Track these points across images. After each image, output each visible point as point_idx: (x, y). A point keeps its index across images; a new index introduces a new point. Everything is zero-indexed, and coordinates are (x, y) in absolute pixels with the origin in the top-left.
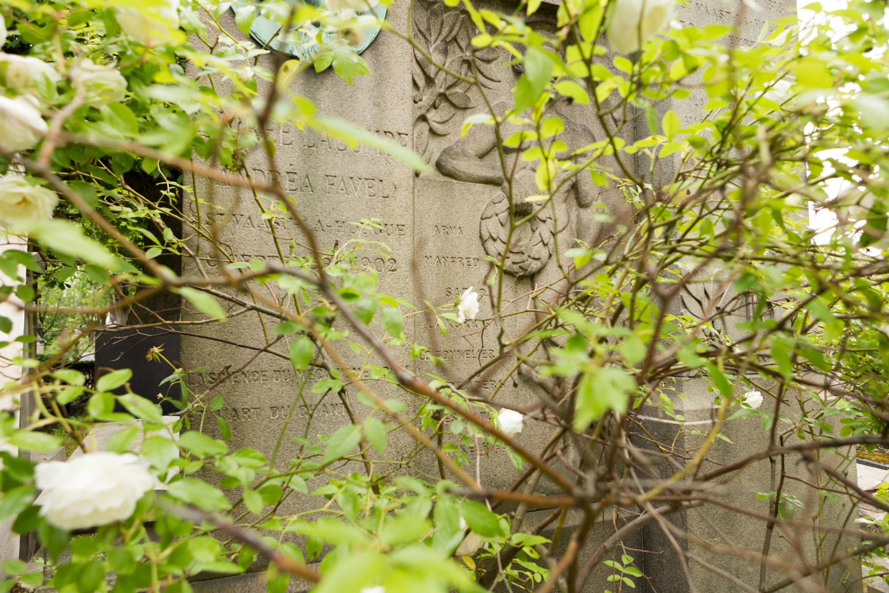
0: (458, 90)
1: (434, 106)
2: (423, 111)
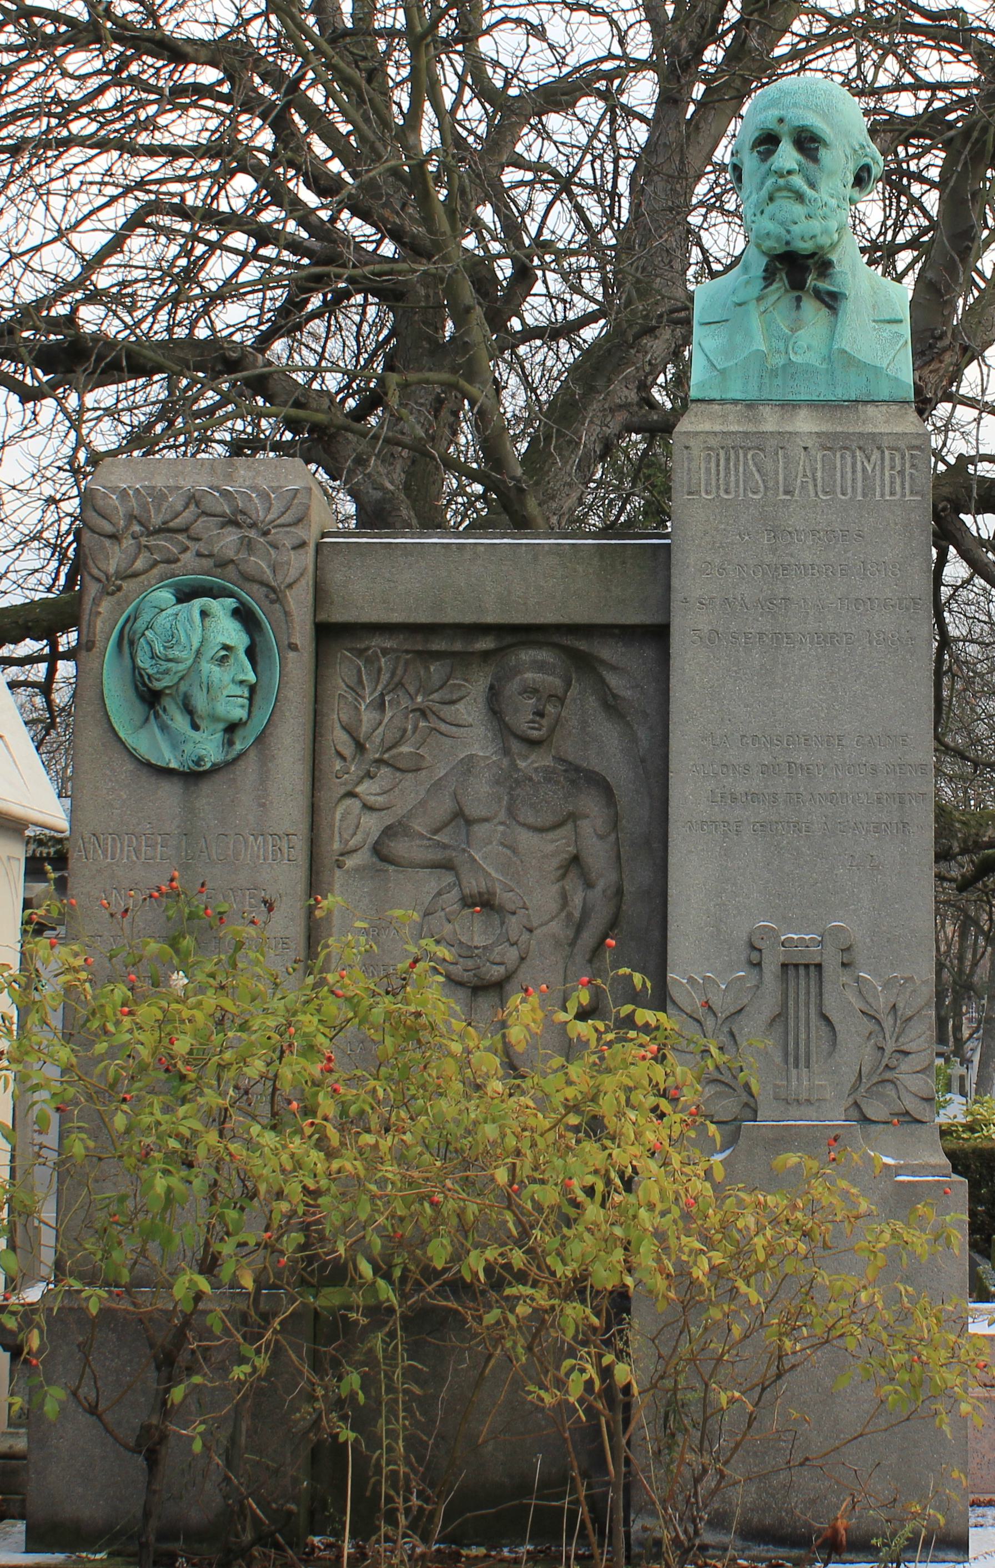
0: (405, 749)
1: (369, 775)
2: (349, 788)
